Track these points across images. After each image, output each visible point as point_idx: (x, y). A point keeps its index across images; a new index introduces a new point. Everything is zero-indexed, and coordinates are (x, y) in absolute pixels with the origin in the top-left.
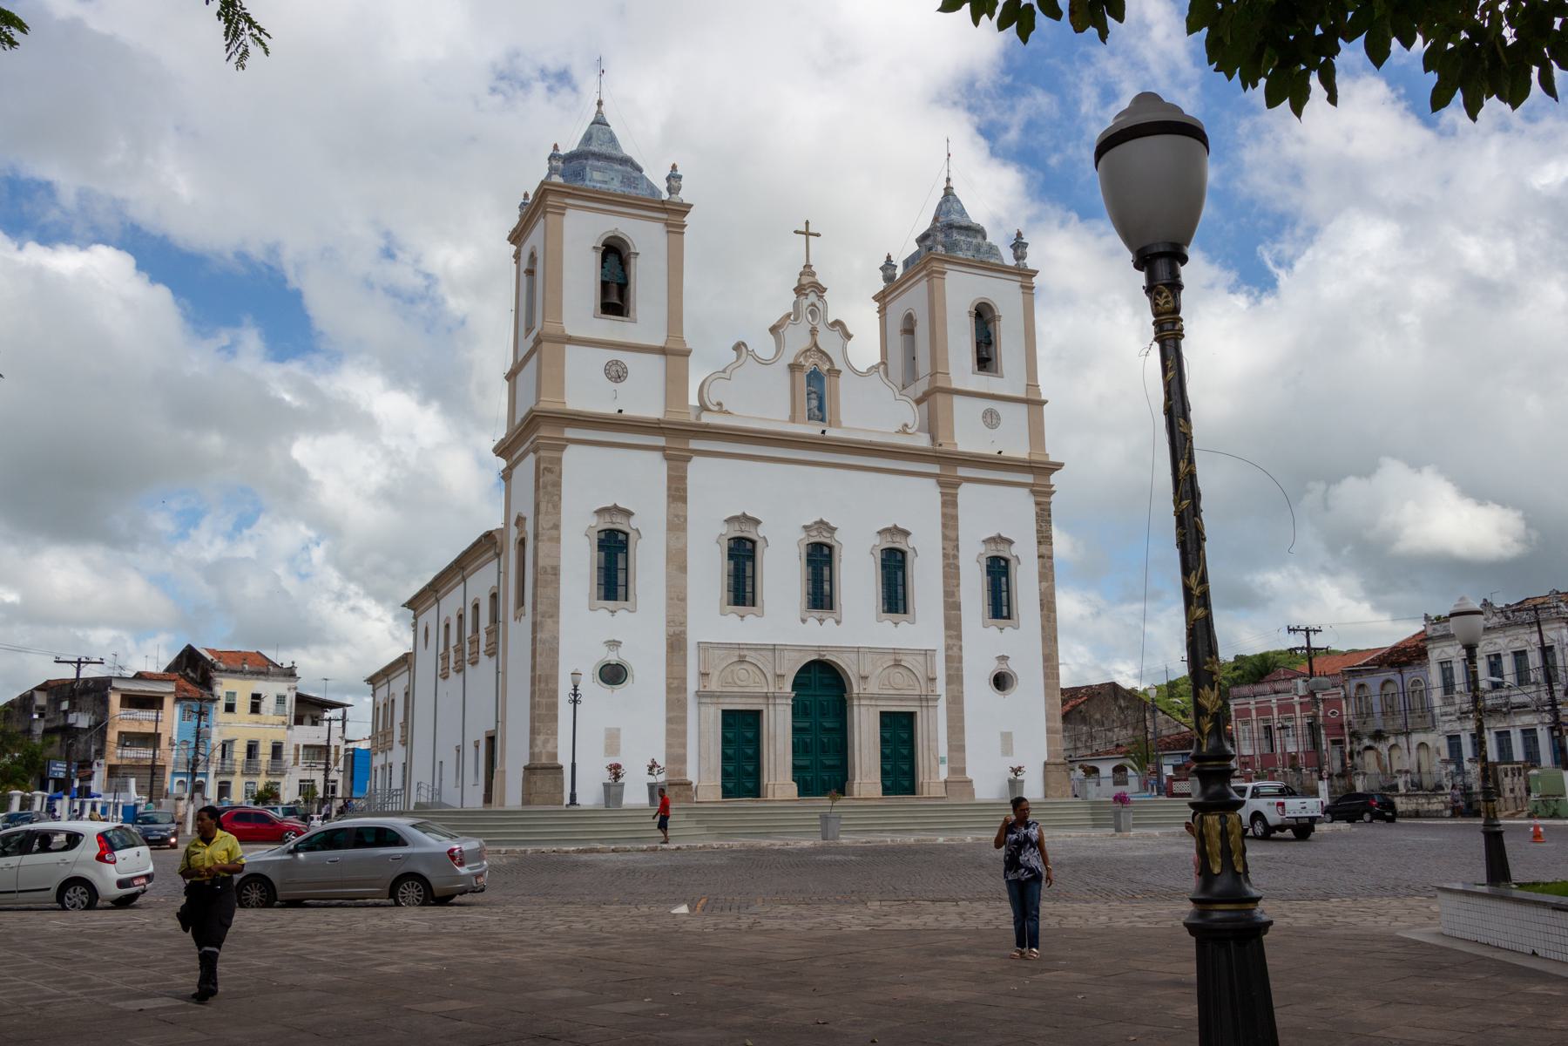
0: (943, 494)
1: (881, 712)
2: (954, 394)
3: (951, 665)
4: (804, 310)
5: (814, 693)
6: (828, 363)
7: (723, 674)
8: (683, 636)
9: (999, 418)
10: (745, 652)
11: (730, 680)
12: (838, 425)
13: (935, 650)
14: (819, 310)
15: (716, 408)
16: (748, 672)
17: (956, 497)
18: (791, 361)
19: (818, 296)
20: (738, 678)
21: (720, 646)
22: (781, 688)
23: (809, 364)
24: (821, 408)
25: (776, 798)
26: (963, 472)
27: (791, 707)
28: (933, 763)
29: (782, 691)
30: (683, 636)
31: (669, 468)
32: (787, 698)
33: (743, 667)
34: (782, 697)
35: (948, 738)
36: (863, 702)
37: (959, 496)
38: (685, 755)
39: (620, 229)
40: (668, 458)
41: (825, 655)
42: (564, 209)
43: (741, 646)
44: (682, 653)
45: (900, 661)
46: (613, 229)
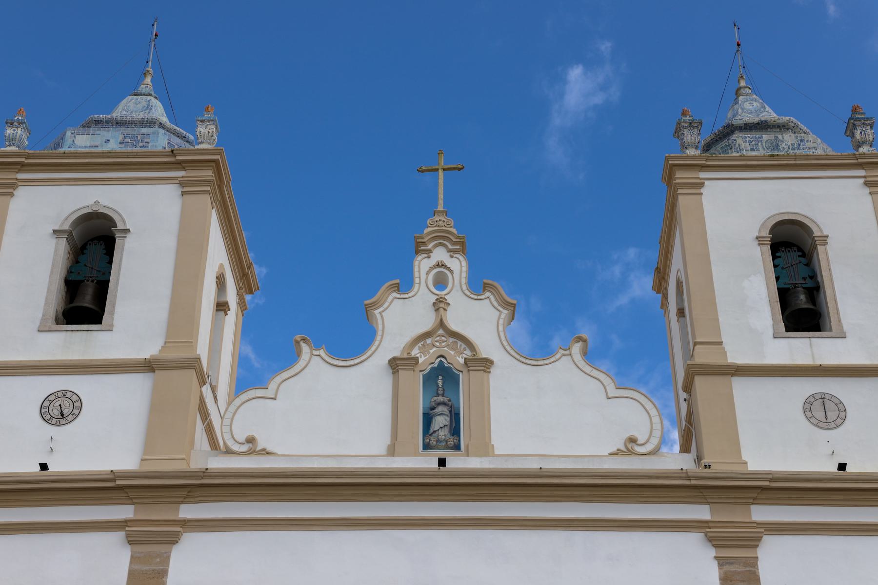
0: (722, 561)
2: (733, 375)
4: (423, 276)
6: (468, 353)
9: (841, 409)
12: (486, 450)
14: (451, 272)
15: (244, 448)
17: (755, 565)
18: (397, 354)
19: (449, 251)
23: (426, 359)
24: (455, 431)
26: (762, 513)
31: (133, 559)
37: (760, 564)
39: (104, 202)
40: (132, 541)
42: (14, 186)
46: (90, 202)
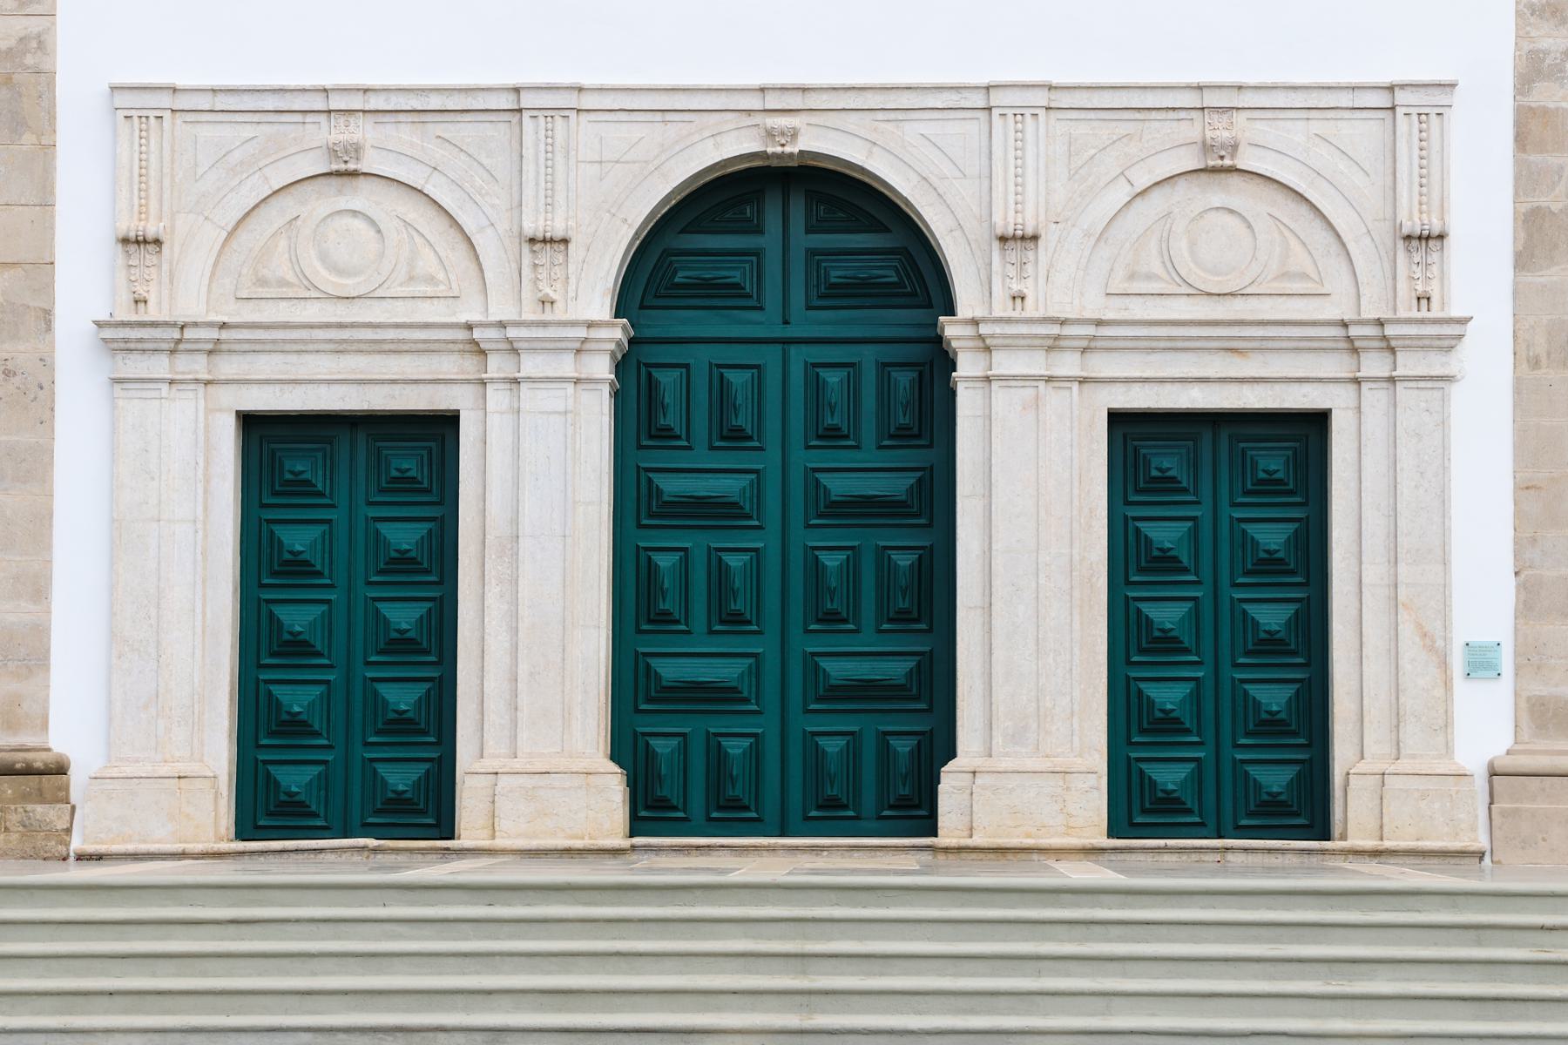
1: (1117, 419)
3: (1534, 158)
5: (779, 332)
7: (243, 237)
8: (29, 60)
10: (361, 131)
11: (280, 267)
13: (1453, 85)
16: (372, 222)
20: (324, 257)
21: (222, 102)
22: (545, 302)
25: (499, 843)
27: (606, 389)
28: (1418, 672)
29: (559, 314)
30: (29, 60)
32: (581, 349)
33: (344, 202)
34: (554, 347)
35: (1524, 544)
36: (1005, 363)
38: (41, 632)
41: (794, 135)
43: (337, 103)
44: (28, 138)
45: (1234, 148)
